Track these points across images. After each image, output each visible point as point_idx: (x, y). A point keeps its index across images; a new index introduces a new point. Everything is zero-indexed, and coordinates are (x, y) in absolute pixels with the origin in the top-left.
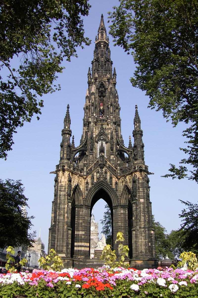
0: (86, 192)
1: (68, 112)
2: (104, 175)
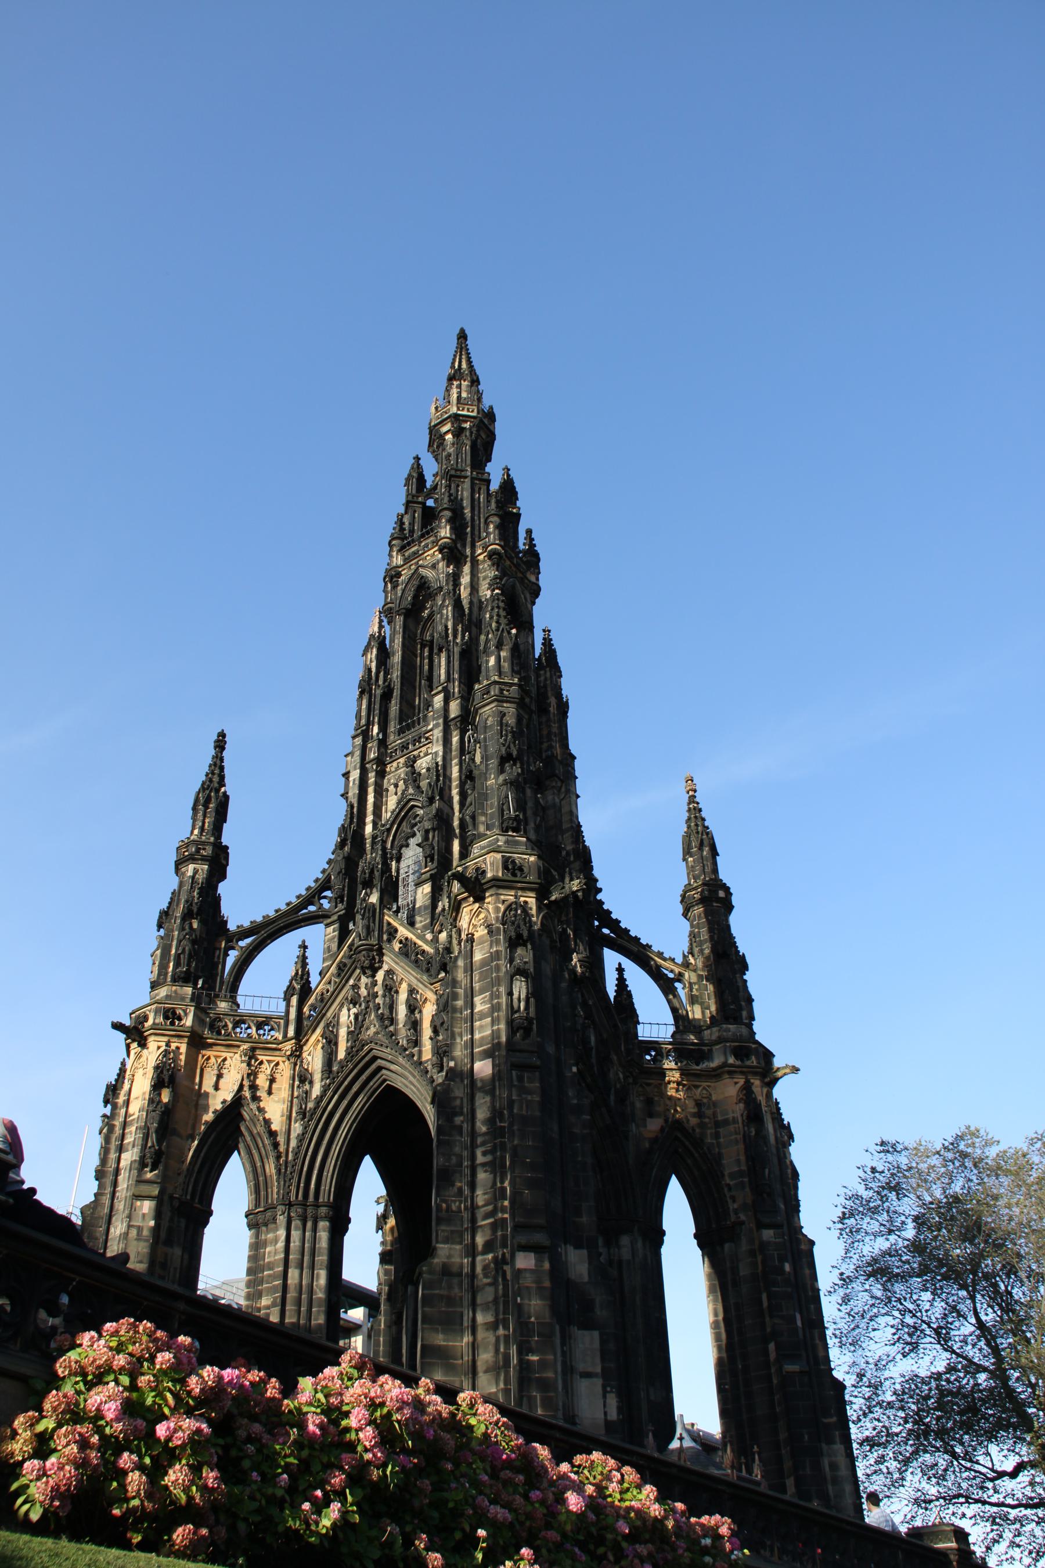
0: (297, 1128)
1: (218, 767)
2: (378, 1007)
